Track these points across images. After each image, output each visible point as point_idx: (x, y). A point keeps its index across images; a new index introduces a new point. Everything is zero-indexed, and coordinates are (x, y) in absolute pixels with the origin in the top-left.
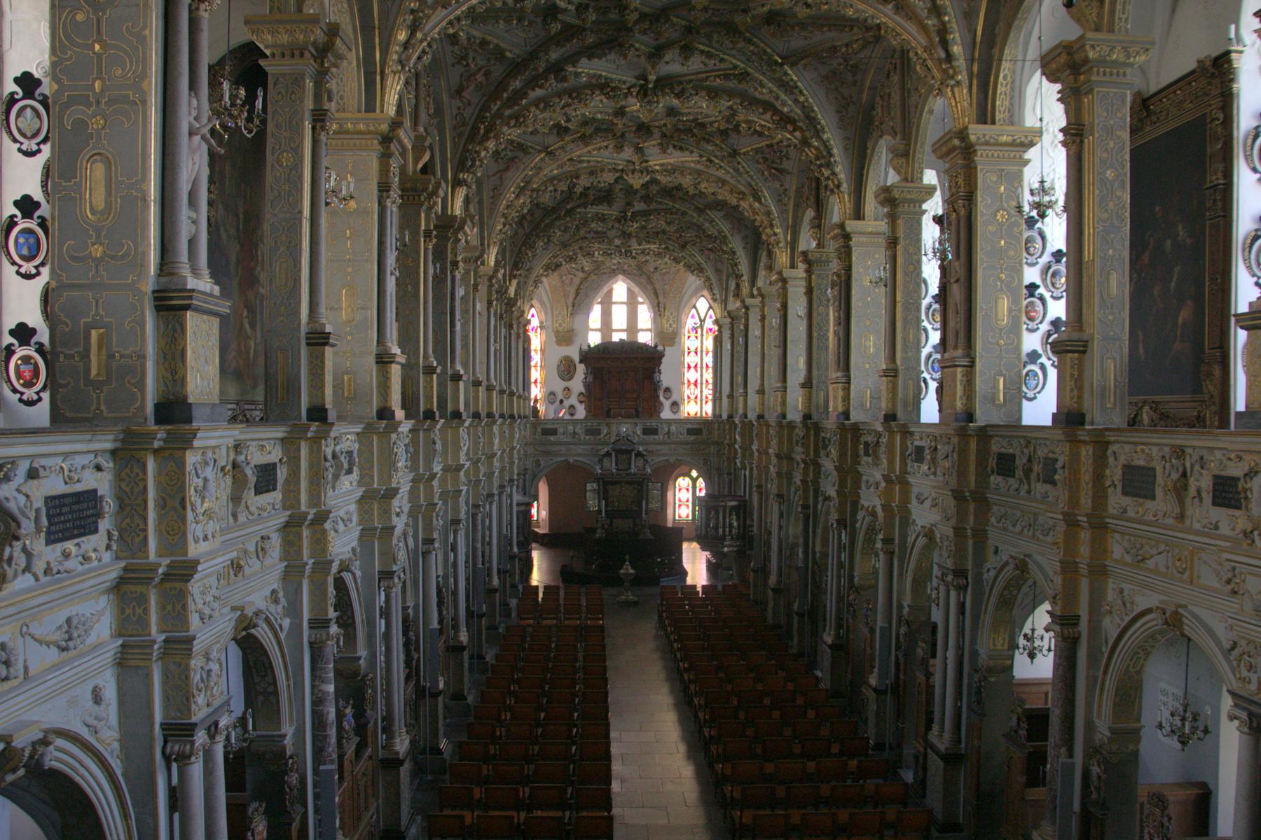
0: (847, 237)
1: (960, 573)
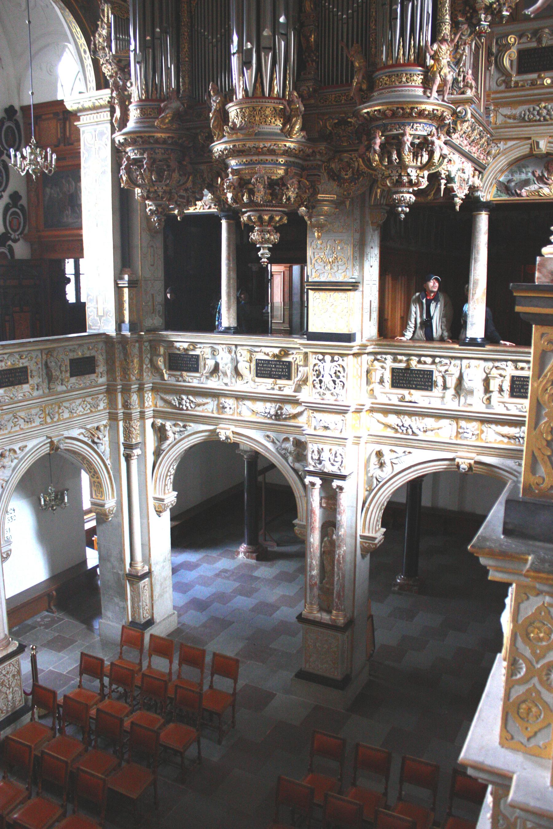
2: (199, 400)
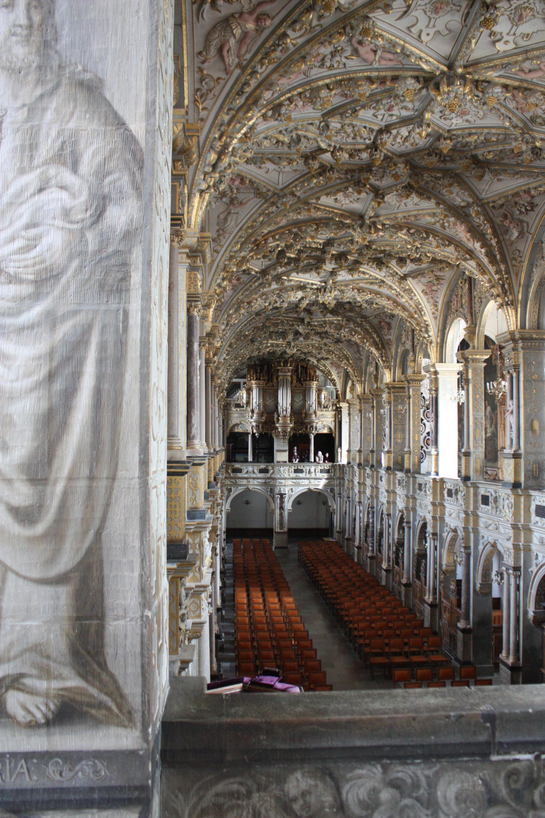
0: (436, 373)
1: (516, 569)
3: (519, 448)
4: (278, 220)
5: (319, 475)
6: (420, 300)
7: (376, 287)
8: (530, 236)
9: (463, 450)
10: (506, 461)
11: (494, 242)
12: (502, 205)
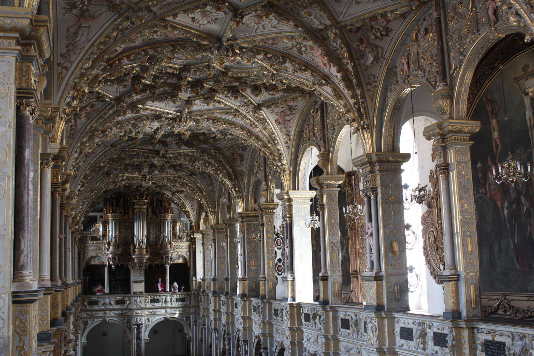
0: (290, 200)
2: (98, 312)
3: (380, 270)
4: (133, 37)
5: (175, 304)
6: (274, 129)
7: (230, 117)
8: (385, 61)
9: (321, 275)
10: (367, 284)
11: (350, 67)
12: (359, 29)
